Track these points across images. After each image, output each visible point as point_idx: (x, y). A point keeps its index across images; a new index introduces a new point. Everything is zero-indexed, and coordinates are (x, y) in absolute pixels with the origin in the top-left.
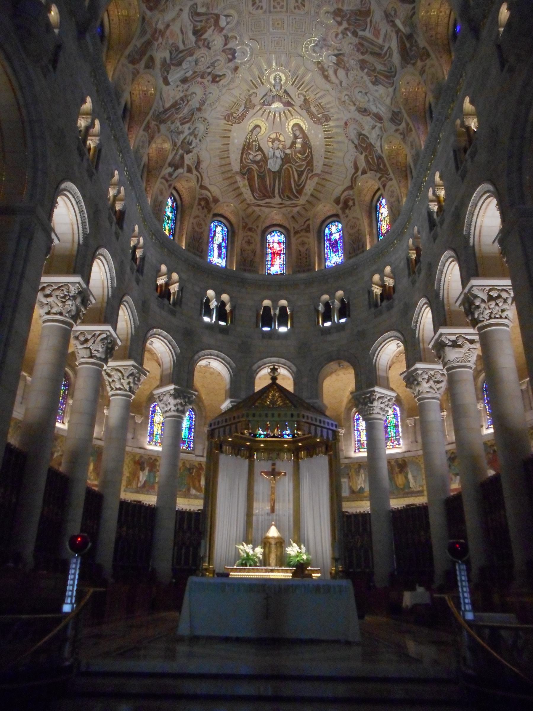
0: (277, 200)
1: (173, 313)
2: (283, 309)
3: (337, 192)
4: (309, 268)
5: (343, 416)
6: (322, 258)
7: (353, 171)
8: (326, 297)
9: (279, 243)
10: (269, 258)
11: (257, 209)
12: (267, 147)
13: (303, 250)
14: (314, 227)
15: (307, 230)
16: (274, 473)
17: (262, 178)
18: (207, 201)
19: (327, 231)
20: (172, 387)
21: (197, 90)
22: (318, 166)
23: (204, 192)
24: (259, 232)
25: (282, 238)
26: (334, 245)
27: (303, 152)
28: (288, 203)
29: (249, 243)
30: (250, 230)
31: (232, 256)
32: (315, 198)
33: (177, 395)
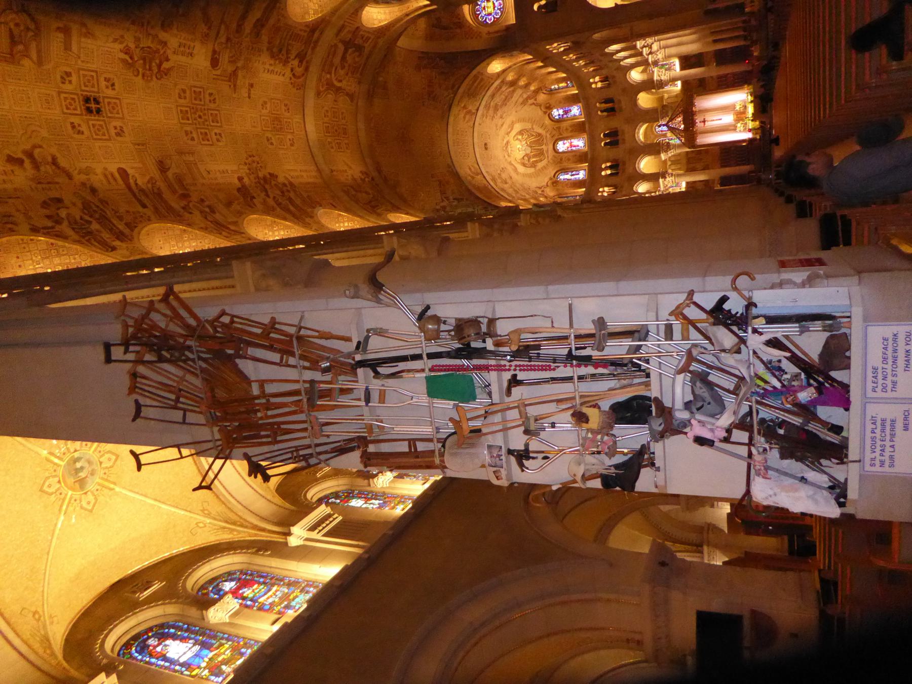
0: (544, 147)
1: (622, 187)
2: (605, 135)
3: (540, 113)
4: (583, 123)
5: (657, 96)
6: (575, 116)
7: (533, 106)
8: (599, 113)
9: (564, 144)
10: (574, 148)
11: (550, 158)
12: (522, 154)
13: (570, 129)
14: (557, 125)
15: (559, 128)
16: (704, 121)
17: (535, 156)
18: (553, 183)
19: (557, 117)
20: (661, 180)
21: (518, 185)
22: (528, 126)
23: (549, 184)
24: (561, 155)
25: (561, 143)
26: (566, 112)
27: (523, 134)
28: (545, 141)
29: (569, 160)
30: (561, 159)
31: (577, 168)
32: (543, 126)
33: (664, 177)
